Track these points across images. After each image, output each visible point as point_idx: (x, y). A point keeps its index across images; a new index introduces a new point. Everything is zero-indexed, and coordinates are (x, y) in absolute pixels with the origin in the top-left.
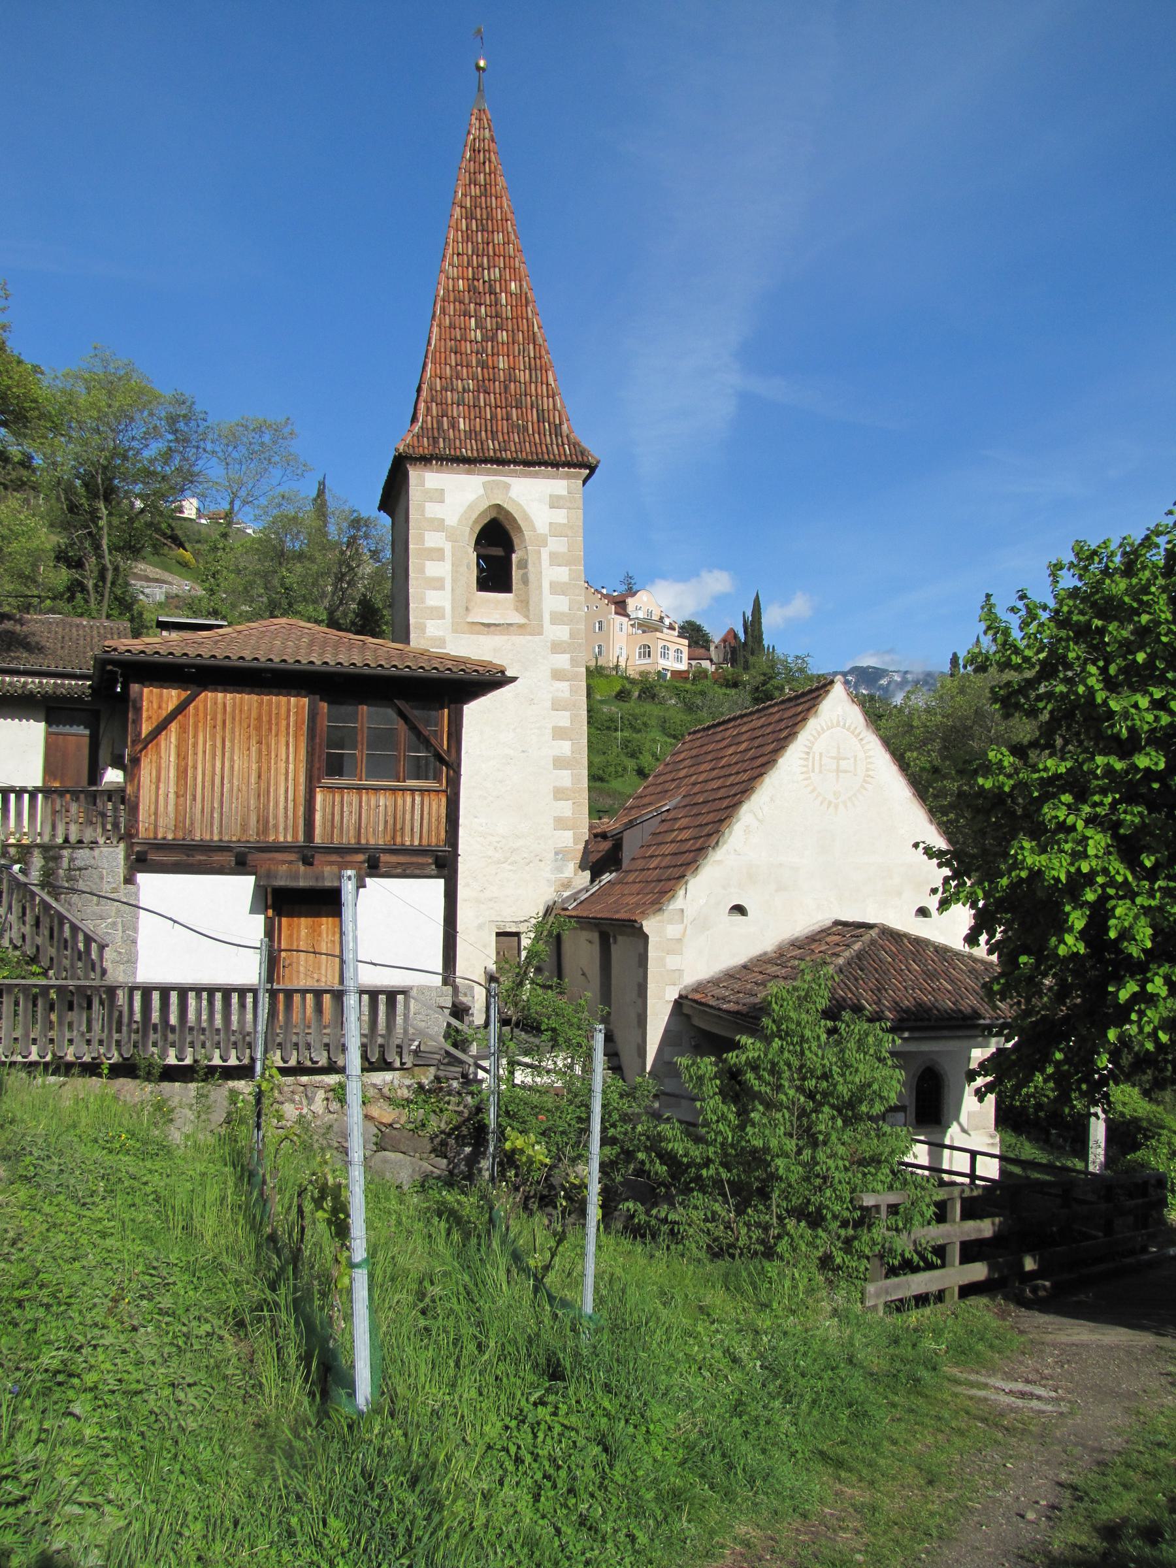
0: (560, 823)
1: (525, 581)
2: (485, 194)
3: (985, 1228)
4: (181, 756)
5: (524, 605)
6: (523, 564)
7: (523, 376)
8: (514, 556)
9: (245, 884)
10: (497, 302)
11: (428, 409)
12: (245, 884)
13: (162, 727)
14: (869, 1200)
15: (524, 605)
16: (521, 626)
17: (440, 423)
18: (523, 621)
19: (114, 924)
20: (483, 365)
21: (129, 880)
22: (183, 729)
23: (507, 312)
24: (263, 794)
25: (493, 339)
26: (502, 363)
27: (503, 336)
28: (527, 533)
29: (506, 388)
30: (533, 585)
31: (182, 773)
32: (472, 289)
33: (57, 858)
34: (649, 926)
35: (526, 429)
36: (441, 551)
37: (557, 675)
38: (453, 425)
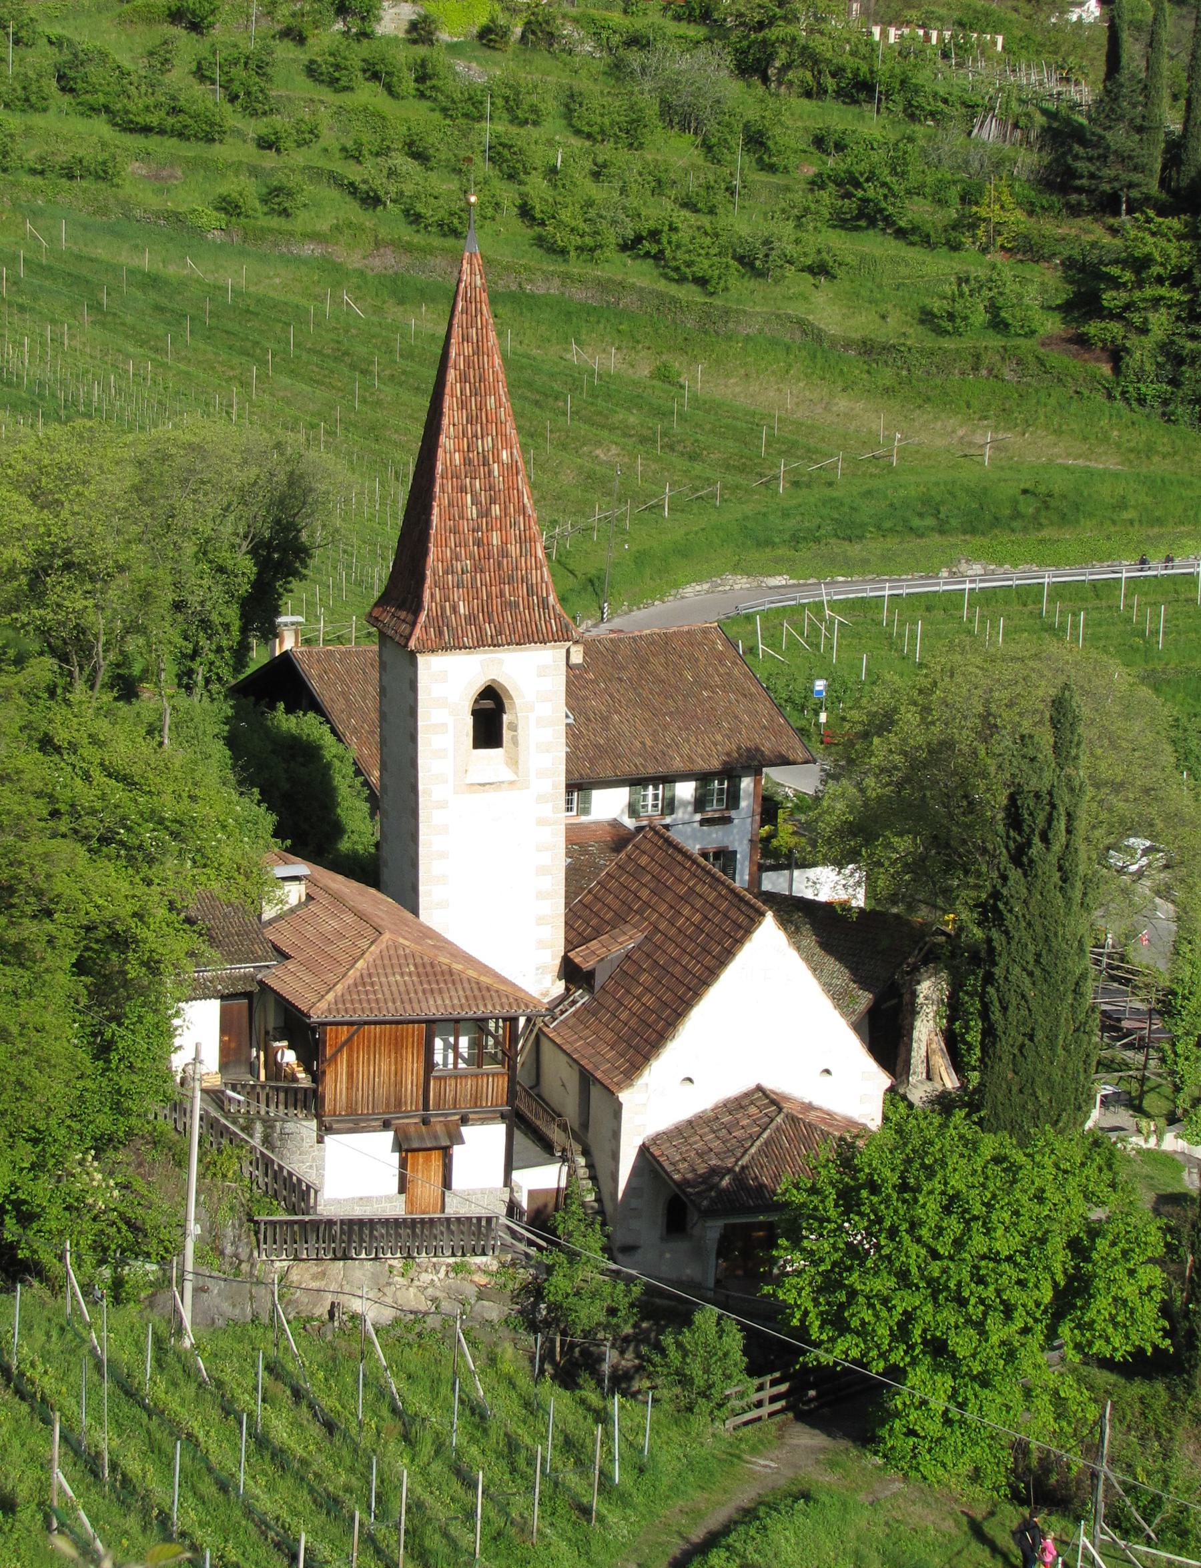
0: (541, 944)
1: (515, 742)
2: (477, 352)
3: (783, 1388)
4: (350, 1065)
5: (513, 762)
6: (514, 728)
7: (513, 549)
8: (505, 717)
9: (389, 1136)
10: (490, 472)
11: (432, 595)
12: (389, 1136)
13: (340, 1050)
14: (727, 1392)
15: (513, 762)
16: (512, 783)
17: (443, 609)
18: (513, 777)
19: (311, 1167)
20: (478, 543)
21: (320, 1141)
22: (351, 1050)
23: (499, 483)
24: (399, 1083)
25: (487, 513)
26: (495, 538)
27: (496, 510)
28: (517, 701)
29: (500, 564)
30: (521, 747)
31: (350, 1075)
32: (467, 462)
33: (272, 1127)
34: (624, 1096)
35: (517, 605)
36: (445, 725)
37: (542, 822)
38: (454, 609)
